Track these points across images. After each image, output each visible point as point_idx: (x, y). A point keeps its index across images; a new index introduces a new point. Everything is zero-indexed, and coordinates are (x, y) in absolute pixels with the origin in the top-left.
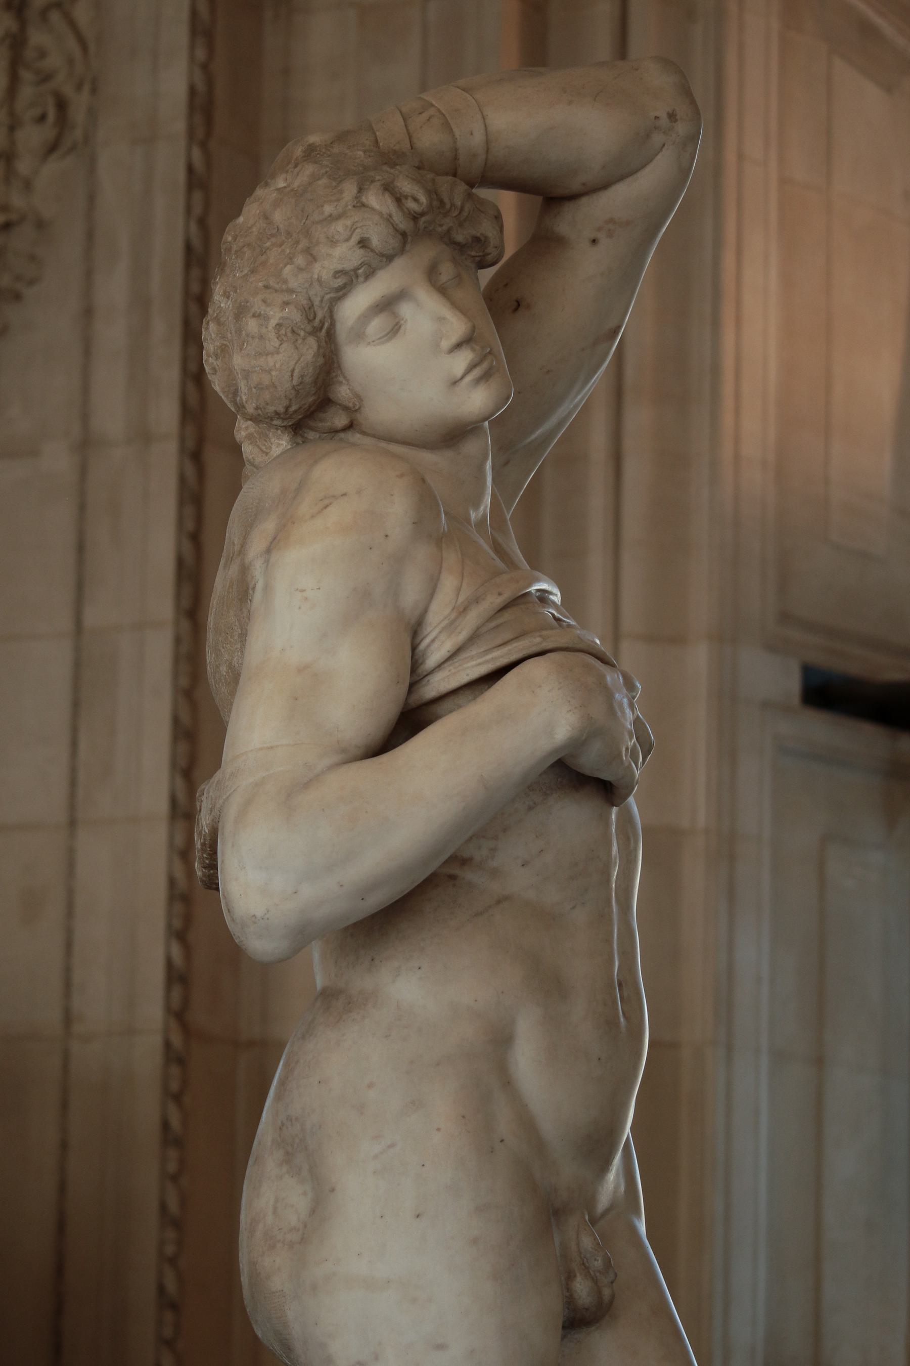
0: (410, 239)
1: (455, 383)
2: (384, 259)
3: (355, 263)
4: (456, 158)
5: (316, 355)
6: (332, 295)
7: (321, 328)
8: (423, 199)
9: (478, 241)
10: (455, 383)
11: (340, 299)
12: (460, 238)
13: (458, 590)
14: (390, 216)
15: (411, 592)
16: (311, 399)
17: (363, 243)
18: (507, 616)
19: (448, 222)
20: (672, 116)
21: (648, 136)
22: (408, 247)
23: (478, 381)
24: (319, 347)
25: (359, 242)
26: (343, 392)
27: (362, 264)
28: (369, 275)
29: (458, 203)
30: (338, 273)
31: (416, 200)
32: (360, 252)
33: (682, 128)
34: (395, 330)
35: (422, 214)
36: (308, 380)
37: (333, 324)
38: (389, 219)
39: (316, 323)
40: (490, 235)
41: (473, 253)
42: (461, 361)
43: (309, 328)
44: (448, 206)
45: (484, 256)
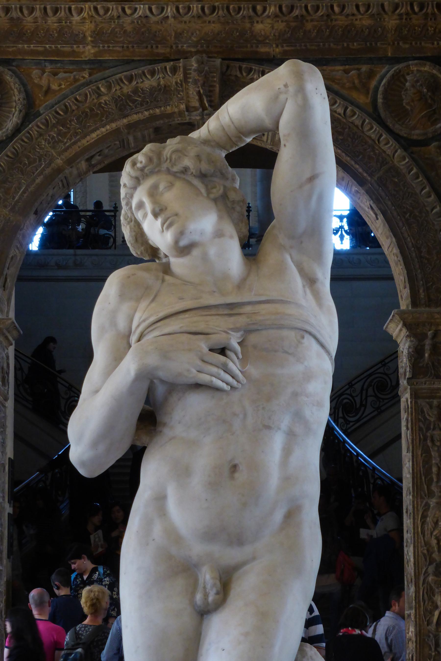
0: (141, 179)
2: (132, 190)
3: (125, 194)
4: (224, 129)
5: (131, 231)
6: (128, 208)
7: (132, 221)
8: (144, 161)
10: (163, 231)
11: (131, 208)
12: (175, 169)
13: (141, 317)
14: (130, 172)
15: (122, 323)
16: (142, 248)
17: (125, 185)
18: (159, 324)
20: (286, 86)
22: (142, 182)
24: (130, 228)
25: (124, 185)
26: (151, 242)
27: (126, 194)
28: (132, 196)
29: (168, 156)
30: (123, 199)
31: (141, 162)
32: (124, 189)
34: (145, 216)
35: (144, 167)
36: (133, 242)
37: (135, 218)
38: (129, 174)
39: (129, 219)
40: (188, 165)
41: (190, 173)
42: (159, 222)
43: (127, 222)
44: (165, 159)
45: (192, 173)
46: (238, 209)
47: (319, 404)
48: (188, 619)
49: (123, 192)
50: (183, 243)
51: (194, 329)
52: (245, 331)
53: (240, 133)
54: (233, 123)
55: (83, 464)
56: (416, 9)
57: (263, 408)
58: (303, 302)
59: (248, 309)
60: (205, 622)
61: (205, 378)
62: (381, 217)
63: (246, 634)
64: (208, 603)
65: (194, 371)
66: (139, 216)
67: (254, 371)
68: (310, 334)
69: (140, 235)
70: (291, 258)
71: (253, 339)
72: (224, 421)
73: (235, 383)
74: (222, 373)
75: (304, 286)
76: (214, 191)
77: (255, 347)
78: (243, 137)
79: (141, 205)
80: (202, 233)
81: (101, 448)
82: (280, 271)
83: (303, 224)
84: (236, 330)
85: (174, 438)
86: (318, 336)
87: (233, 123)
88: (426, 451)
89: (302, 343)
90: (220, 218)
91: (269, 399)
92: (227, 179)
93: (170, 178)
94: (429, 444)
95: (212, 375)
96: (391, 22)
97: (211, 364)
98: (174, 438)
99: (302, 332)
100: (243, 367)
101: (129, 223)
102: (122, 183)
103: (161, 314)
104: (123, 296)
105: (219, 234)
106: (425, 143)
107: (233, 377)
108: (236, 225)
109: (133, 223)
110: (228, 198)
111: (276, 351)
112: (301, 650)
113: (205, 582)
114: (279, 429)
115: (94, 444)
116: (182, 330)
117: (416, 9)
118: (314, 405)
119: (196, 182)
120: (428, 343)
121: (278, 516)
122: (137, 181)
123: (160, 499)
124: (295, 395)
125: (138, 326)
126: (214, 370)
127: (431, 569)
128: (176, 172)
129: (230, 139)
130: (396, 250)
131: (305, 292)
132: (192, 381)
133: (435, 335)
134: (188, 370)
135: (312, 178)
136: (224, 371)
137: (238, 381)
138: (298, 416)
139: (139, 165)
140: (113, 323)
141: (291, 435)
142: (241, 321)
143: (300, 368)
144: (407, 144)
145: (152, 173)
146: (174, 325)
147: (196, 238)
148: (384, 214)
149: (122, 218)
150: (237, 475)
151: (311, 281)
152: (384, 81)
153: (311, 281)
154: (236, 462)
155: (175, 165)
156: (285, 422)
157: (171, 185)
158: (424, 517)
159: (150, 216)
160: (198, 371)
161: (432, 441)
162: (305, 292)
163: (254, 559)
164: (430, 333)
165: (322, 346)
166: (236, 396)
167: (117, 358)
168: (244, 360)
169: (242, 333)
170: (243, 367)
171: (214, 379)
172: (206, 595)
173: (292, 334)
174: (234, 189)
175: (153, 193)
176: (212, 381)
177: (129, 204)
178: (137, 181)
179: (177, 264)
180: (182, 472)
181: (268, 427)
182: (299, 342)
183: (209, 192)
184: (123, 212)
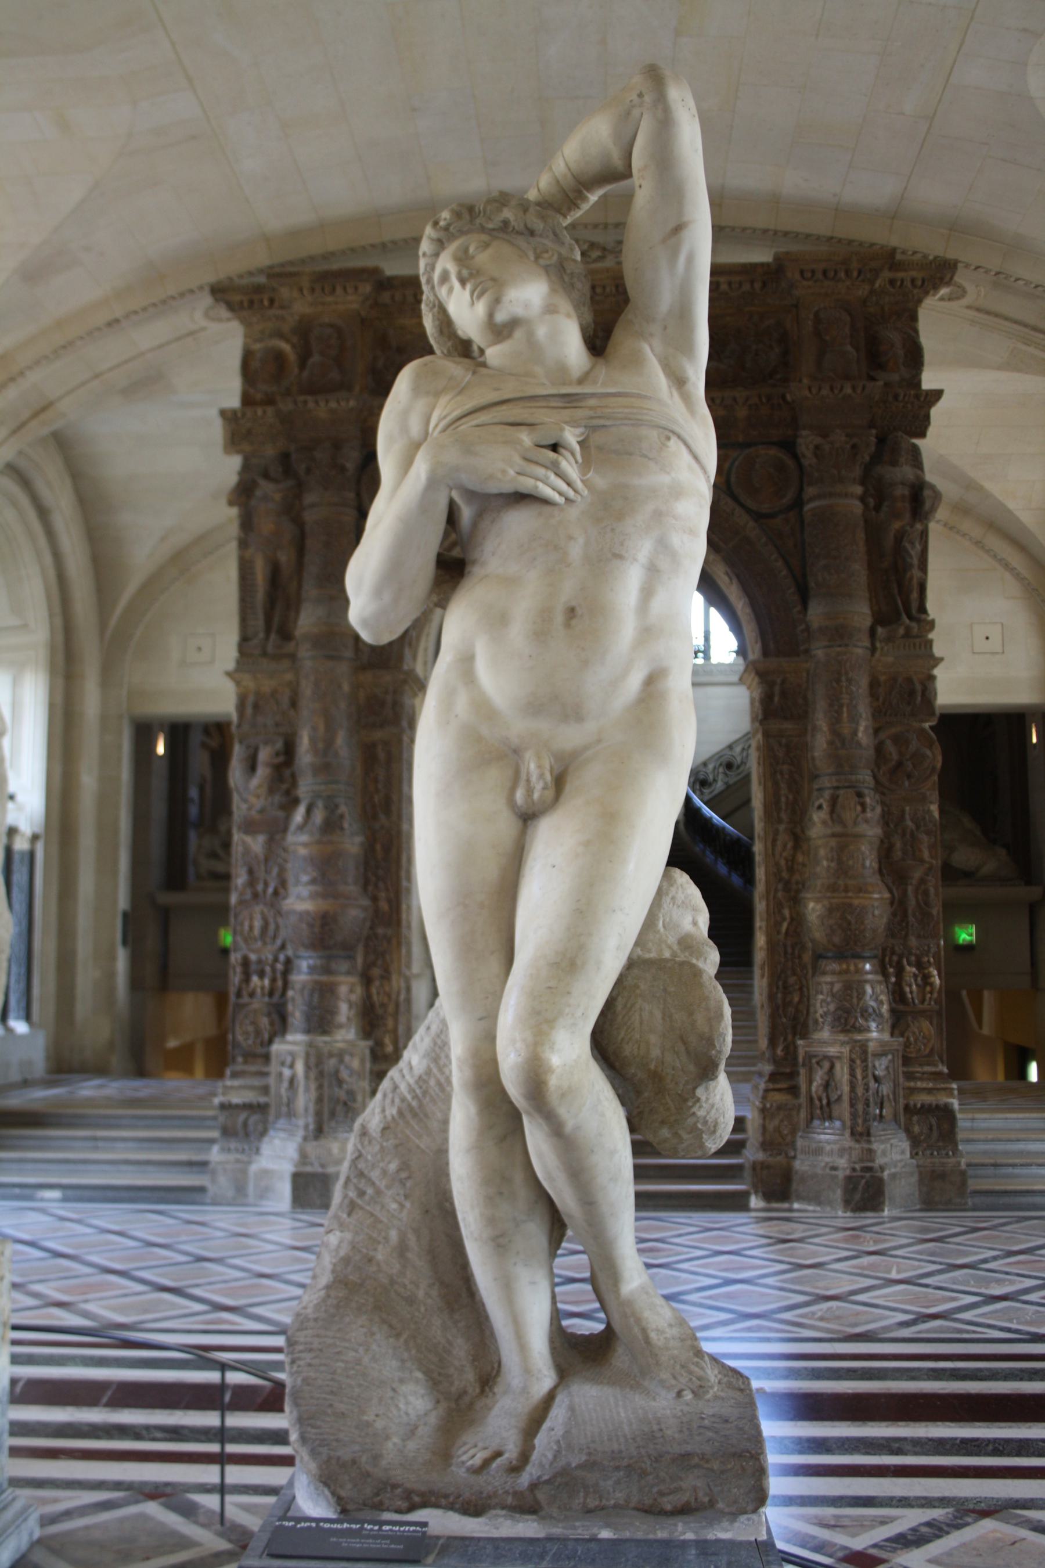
1: (473, 304)
4: (558, 182)
5: (433, 321)
9: (506, 223)
10: (473, 304)
11: (433, 288)
12: (491, 226)
16: (449, 344)
17: (424, 254)
18: (464, 420)
19: (478, 221)
20: (640, 95)
21: (628, 113)
22: (446, 244)
23: (479, 297)
24: (433, 316)
26: (460, 333)
27: (426, 265)
28: (433, 268)
33: (647, 99)
34: (451, 290)
46: (579, 285)
47: (692, 532)
48: (506, 825)
49: (422, 263)
50: (500, 317)
51: (511, 420)
52: (585, 427)
53: (580, 183)
54: (569, 169)
55: (365, 623)
56: (764, 400)
57: (613, 530)
58: (669, 402)
59: (592, 402)
60: (529, 832)
61: (526, 484)
62: (735, 581)
63: (587, 844)
64: (533, 803)
65: (512, 472)
66: (442, 292)
67: (600, 482)
68: (679, 437)
69: (446, 323)
70: (652, 351)
71: (597, 439)
72: (556, 548)
73: (571, 494)
74: (552, 477)
75: (669, 387)
76: (546, 255)
77: (600, 448)
78: (585, 192)
79: (445, 277)
80: (527, 306)
81: (387, 597)
82: (636, 362)
83: (665, 300)
84: (574, 423)
85: (486, 576)
86: (690, 441)
87: (569, 169)
88: (776, 784)
89: (667, 447)
90: (553, 290)
91: (620, 516)
92: (563, 243)
93: (484, 237)
94: (779, 777)
95: (537, 479)
96: (742, 413)
97: (537, 463)
98: (486, 576)
99: (667, 433)
100: (584, 475)
101: (431, 309)
102: (421, 253)
103: (469, 406)
104: (417, 390)
105: (550, 309)
106: (771, 516)
107: (569, 484)
108: (577, 307)
109: (436, 310)
110: (565, 270)
111: (631, 454)
112: (666, 875)
113: (528, 773)
114: (635, 560)
115: (377, 593)
116: (496, 420)
117: (764, 400)
118: (684, 532)
119: (521, 241)
120: (777, 689)
121: (634, 682)
122: (440, 244)
123: (466, 661)
124: (658, 515)
125: (436, 426)
126: (541, 471)
127: (780, 886)
128: (494, 230)
129: (567, 196)
130: (748, 610)
131: (671, 393)
132: (507, 488)
133: (783, 682)
134: (504, 472)
135: (678, 229)
136: (557, 474)
137: (576, 491)
138: (663, 545)
139: (442, 223)
140: (404, 428)
141: (653, 571)
142: (580, 413)
143: (664, 479)
144: (759, 517)
145: (462, 233)
146: (483, 418)
147: (519, 311)
148: (738, 576)
149: (423, 306)
150: (574, 622)
151: (679, 382)
152: (737, 463)
153: (679, 382)
154: (574, 603)
155: (490, 219)
156: (643, 549)
157: (487, 245)
158: (774, 841)
159: (457, 285)
160: (518, 473)
161: (782, 774)
162: (671, 393)
163: (599, 741)
164: (779, 681)
165: (696, 458)
166: (573, 513)
167: (407, 464)
168: (585, 465)
169: (582, 430)
170: (584, 475)
171: (540, 485)
172: (530, 791)
173: (654, 434)
174: (575, 261)
175: (463, 259)
176: (537, 487)
177: (429, 281)
178: (440, 244)
179: (494, 354)
180: (496, 621)
181: (619, 557)
182: (664, 445)
183: (537, 257)
184: (424, 297)
